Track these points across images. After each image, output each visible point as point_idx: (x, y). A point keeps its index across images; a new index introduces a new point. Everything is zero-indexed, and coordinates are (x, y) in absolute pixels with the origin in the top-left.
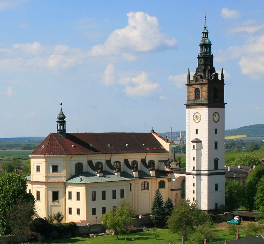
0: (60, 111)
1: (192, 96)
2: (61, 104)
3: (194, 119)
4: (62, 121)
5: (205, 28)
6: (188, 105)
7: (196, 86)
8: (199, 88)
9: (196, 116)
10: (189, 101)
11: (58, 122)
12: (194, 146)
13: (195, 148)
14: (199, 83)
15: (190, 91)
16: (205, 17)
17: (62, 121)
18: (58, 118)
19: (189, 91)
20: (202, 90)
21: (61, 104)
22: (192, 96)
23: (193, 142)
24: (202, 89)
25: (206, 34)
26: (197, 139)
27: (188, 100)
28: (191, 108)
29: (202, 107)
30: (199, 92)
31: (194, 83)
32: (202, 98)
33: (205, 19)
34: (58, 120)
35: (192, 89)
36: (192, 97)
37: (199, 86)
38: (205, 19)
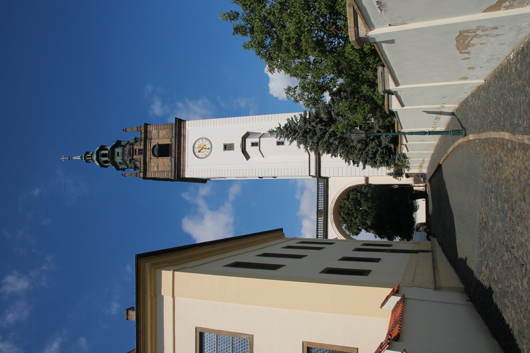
3: (204, 156)
7: (149, 153)
8: (153, 144)
9: (199, 151)
12: (253, 144)
15: (156, 169)
23: (247, 157)
28: (184, 166)
29: (184, 137)
30: (160, 146)
36: (166, 164)
37: (148, 147)
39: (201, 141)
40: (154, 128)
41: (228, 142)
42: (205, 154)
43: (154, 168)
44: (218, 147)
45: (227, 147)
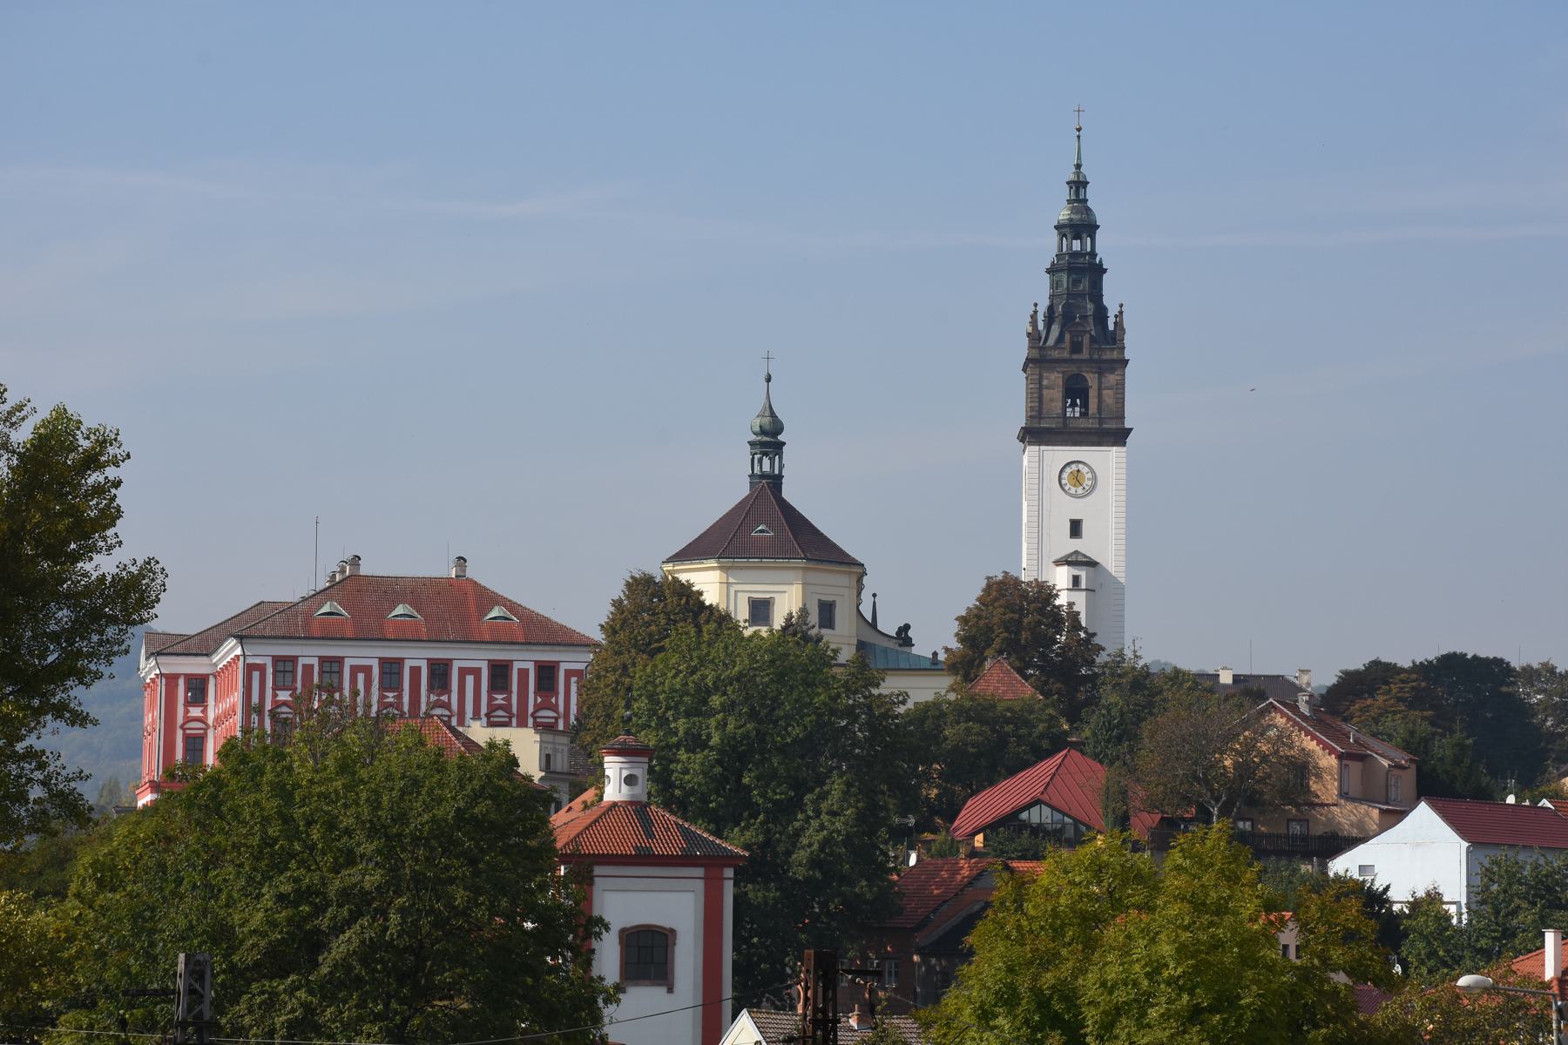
0: (763, 400)
1: (1052, 400)
2: (769, 379)
3: (1063, 482)
4: (769, 441)
5: (1078, 166)
6: (1033, 434)
10: (1040, 418)
11: (752, 444)
13: (1083, 586)
14: (1085, 355)
15: (1045, 382)
16: (1079, 130)
17: (769, 441)
18: (757, 429)
19: (1040, 383)
20: (1100, 383)
21: (769, 379)
22: (1052, 400)
23: (1058, 563)
24: (1100, 379)
25: (1079, 185)
26: (1076, 552)
27: (1033, 413)
31: (1066, 355)
32: (1100, 410)
33: (1079, 137)
34: (753, 438)
35: (1055, 379)
36: (1053, 404)
38: (1079, 137)
39: (1090, 475)
40: (1118, 378)
41: (1085, 528)
42: (1066, 484)
43: (1047, 378)
44: (1076, 509)
45: (1076, 528)
